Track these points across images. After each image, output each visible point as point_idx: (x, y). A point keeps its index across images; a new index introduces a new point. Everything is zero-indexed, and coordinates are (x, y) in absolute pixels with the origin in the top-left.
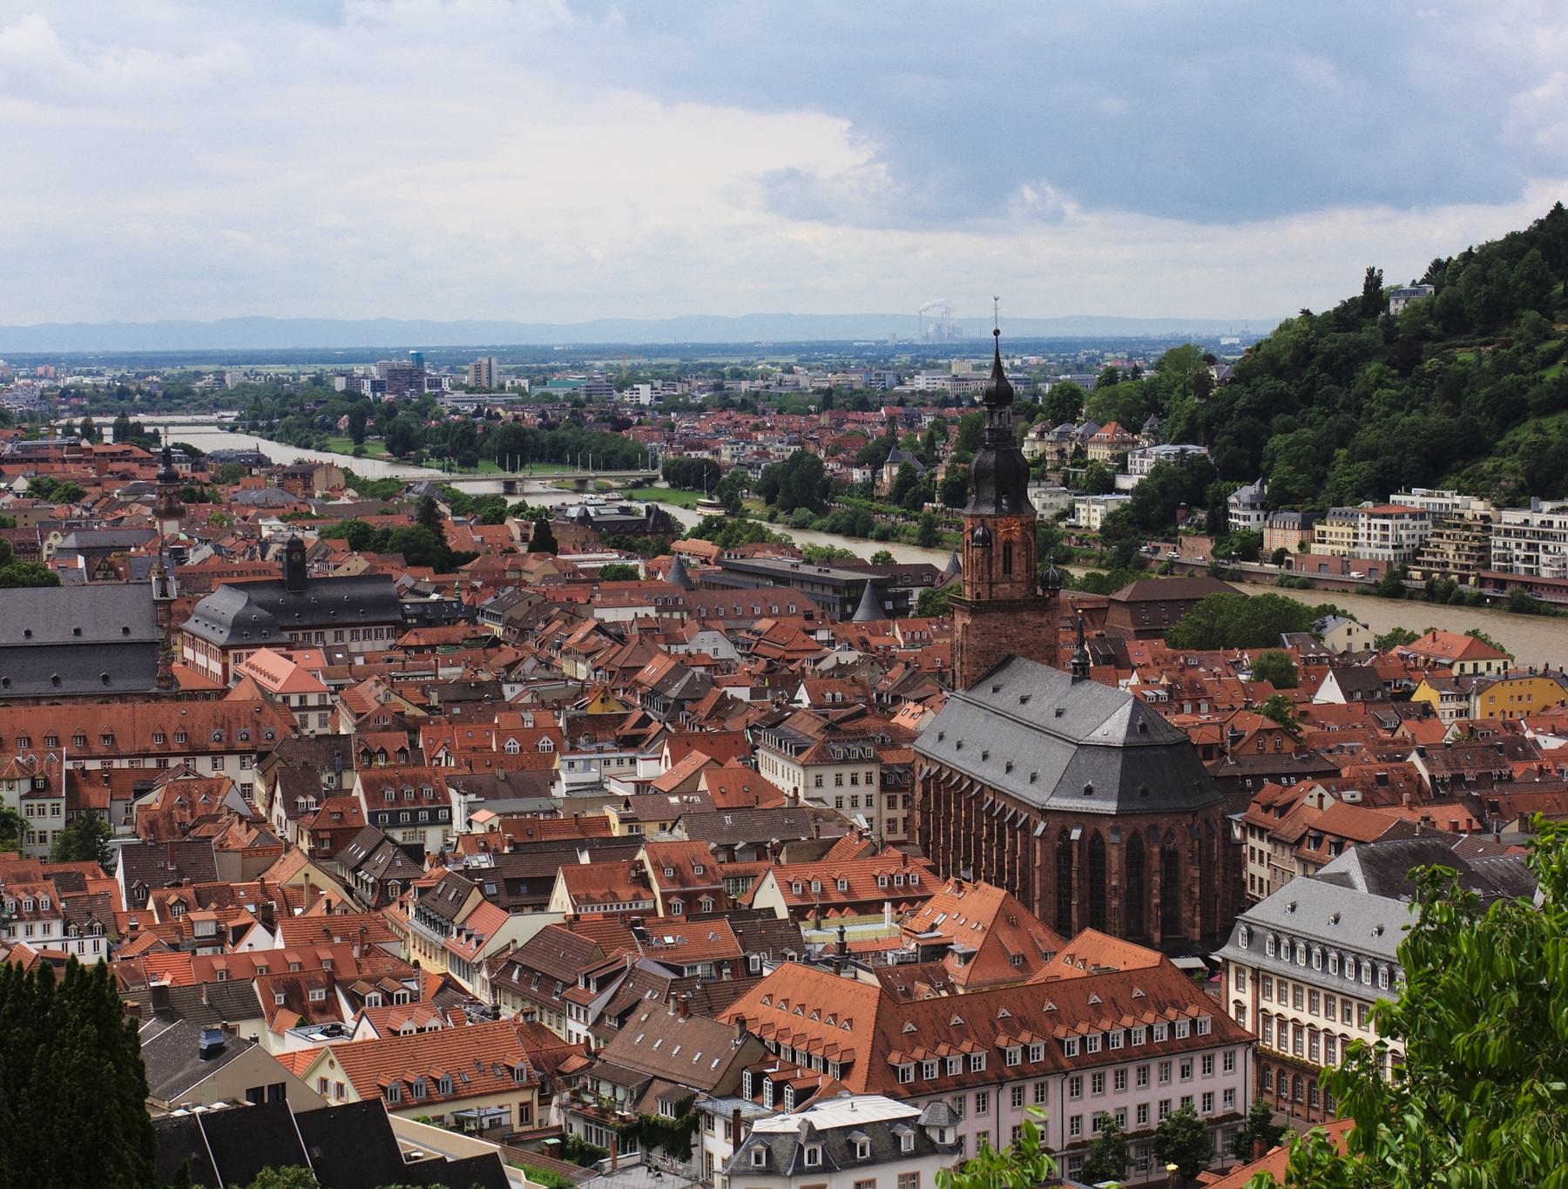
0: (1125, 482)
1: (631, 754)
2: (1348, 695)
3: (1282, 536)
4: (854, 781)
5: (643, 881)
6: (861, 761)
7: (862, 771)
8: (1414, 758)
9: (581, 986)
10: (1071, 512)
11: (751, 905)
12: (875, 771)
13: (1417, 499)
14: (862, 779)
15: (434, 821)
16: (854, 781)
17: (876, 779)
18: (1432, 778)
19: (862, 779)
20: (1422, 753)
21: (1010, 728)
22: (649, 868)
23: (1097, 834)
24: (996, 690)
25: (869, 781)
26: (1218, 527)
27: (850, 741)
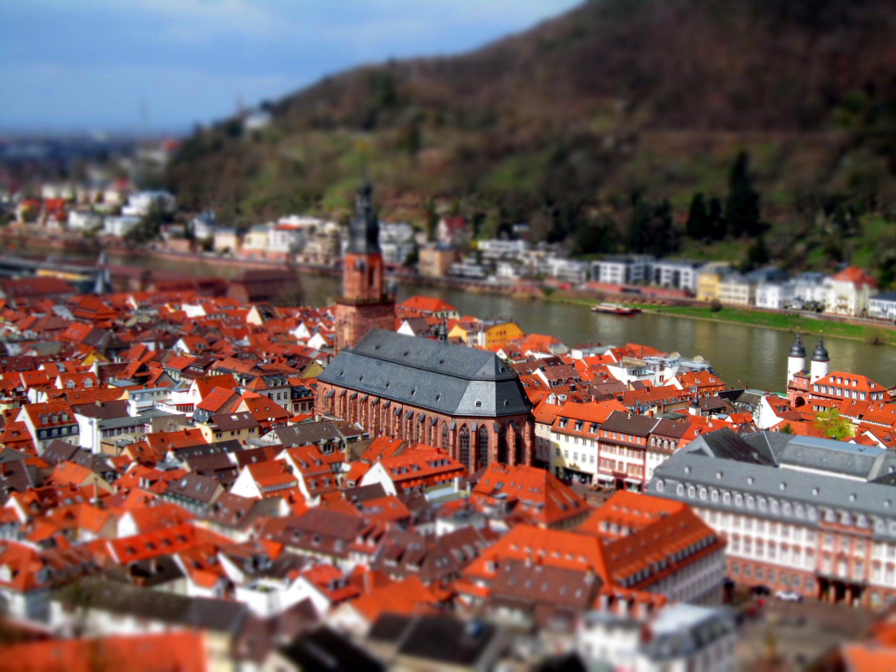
0: (126, 211)
1: (164, 389)
2: (417, 332)
3: (225, 240)
4: (279, 398)
5: (289, 470)
6: (283, 386)
7: (282, 392)
8: (538, 372)
9: (359, 541)
10: (101, 227)
11: (358, 481)
12: (288, 391)
13: (294, 221)
14: (282, 396)
15: (70, 433)
16: (279, 398)
17: (289, 395)
18: (549, 382)
19: (282, 396)
20: (543, 370)
21: (402, 369)
22: (290, 462)
23: (483, 426)
24: (377, 348)
25: (285, 397)
26: (189, 236)
27: (276, 375)
